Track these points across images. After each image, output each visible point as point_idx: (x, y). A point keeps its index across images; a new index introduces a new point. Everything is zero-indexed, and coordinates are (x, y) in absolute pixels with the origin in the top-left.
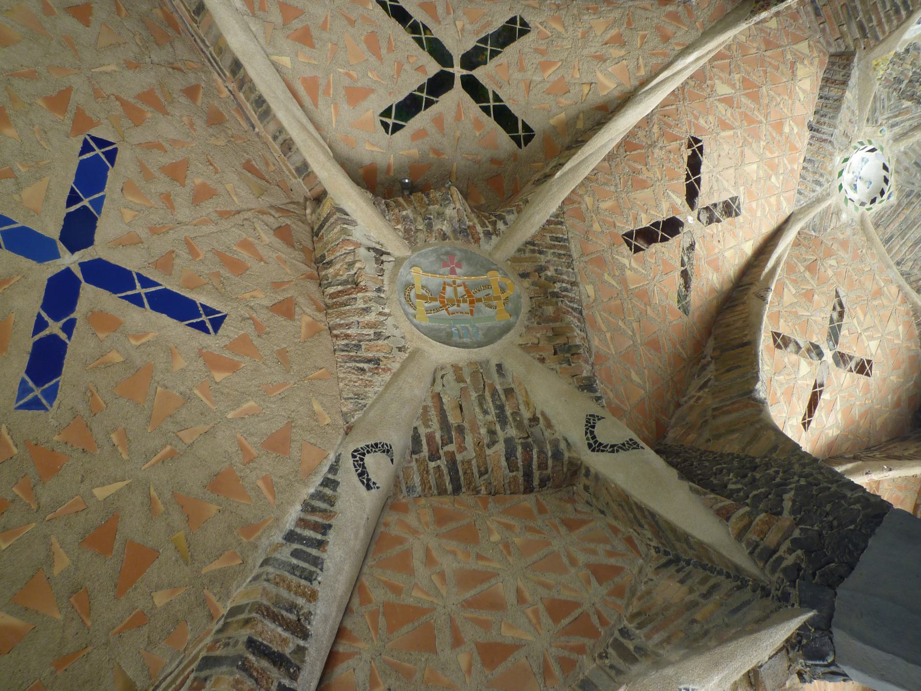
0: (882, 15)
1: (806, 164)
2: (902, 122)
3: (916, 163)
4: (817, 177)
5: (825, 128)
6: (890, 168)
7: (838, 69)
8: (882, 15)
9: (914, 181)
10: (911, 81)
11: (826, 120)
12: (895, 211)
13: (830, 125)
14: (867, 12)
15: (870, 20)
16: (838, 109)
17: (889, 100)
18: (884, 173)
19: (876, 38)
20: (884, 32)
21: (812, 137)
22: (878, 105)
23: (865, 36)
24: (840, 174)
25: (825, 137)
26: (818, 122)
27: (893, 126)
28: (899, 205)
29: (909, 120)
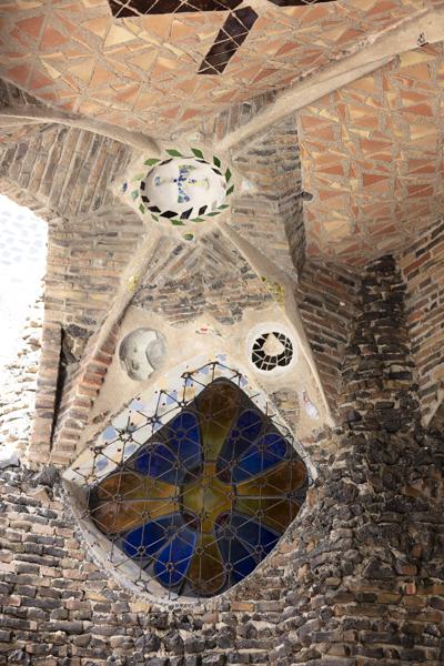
0: (319, 326)
1: (296, 161)
2: (171, 258)
3: (116, 234)
4: (272, 158)
5: (290, 205)
6: (148, 213)
7: (301, 256)
8: (319, 326)
9: (101, 219)
10: (200, 295)
11: (291, 213)
12: (105, 178)
13: (287, 211)
14: (327, 316)
15: (319, 313)
16: (287, 230)
17: (209, 267)
18: (152, 204)
19: (300, 306)
20: (305, 316)
21: (299, 188)
22: (217, 255)
23: (307, 299)
24: (228, 175)
25: (287, 198)
26: (297, 205)
27: (179, 249)
28: (103, 187)
29: (165, 264)
